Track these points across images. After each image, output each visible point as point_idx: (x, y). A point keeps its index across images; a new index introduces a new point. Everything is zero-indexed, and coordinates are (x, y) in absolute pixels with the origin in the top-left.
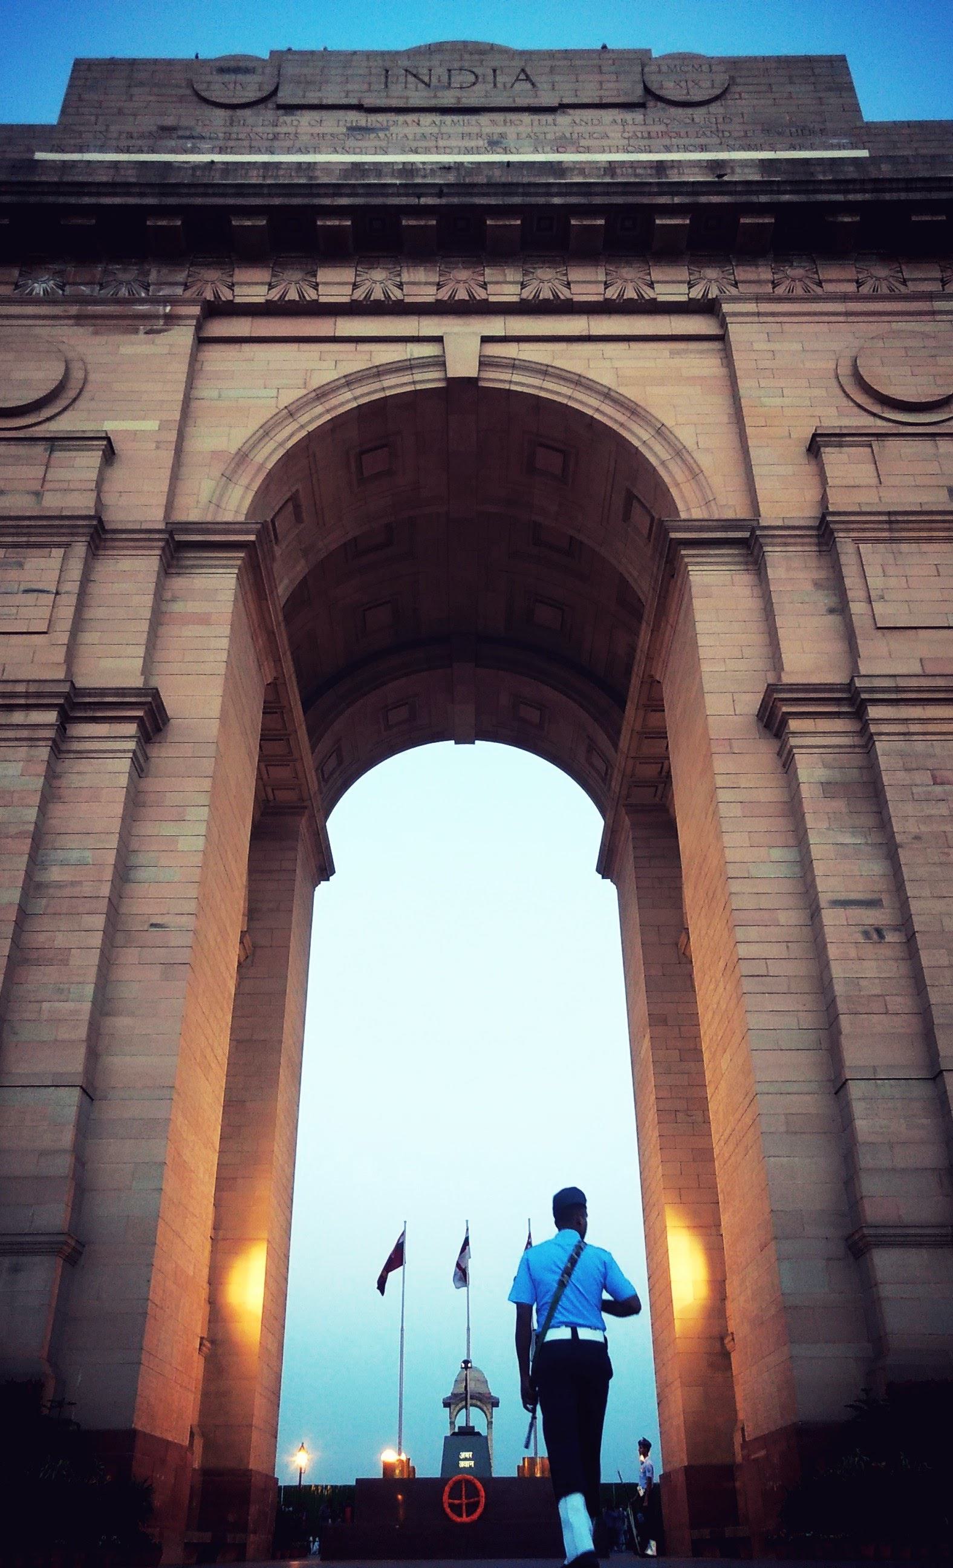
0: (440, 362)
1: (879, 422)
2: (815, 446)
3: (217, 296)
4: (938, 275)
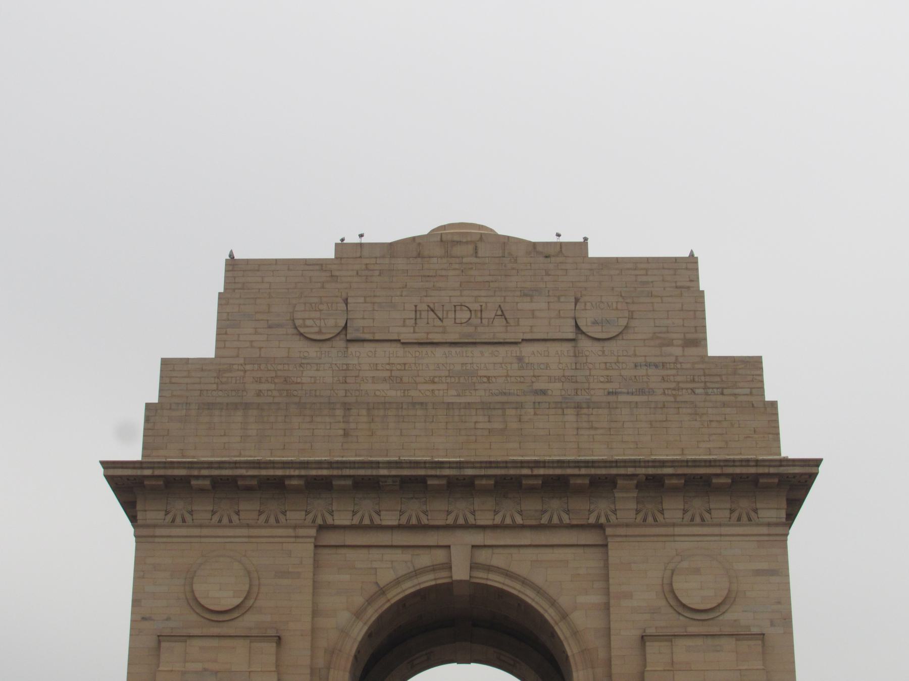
0: (448, 567)
1: (681, 618)
2: (643, 637)
3: (324, 520)
4: (728, 506)
